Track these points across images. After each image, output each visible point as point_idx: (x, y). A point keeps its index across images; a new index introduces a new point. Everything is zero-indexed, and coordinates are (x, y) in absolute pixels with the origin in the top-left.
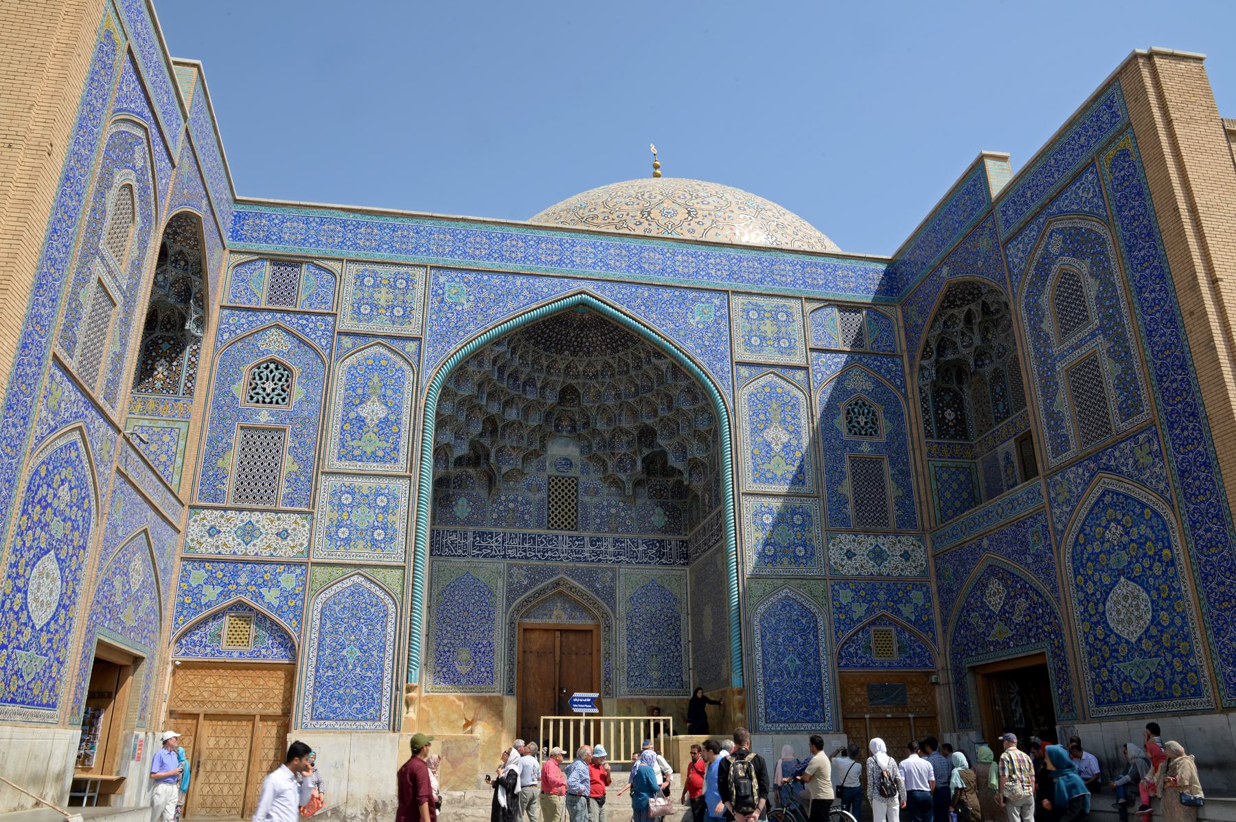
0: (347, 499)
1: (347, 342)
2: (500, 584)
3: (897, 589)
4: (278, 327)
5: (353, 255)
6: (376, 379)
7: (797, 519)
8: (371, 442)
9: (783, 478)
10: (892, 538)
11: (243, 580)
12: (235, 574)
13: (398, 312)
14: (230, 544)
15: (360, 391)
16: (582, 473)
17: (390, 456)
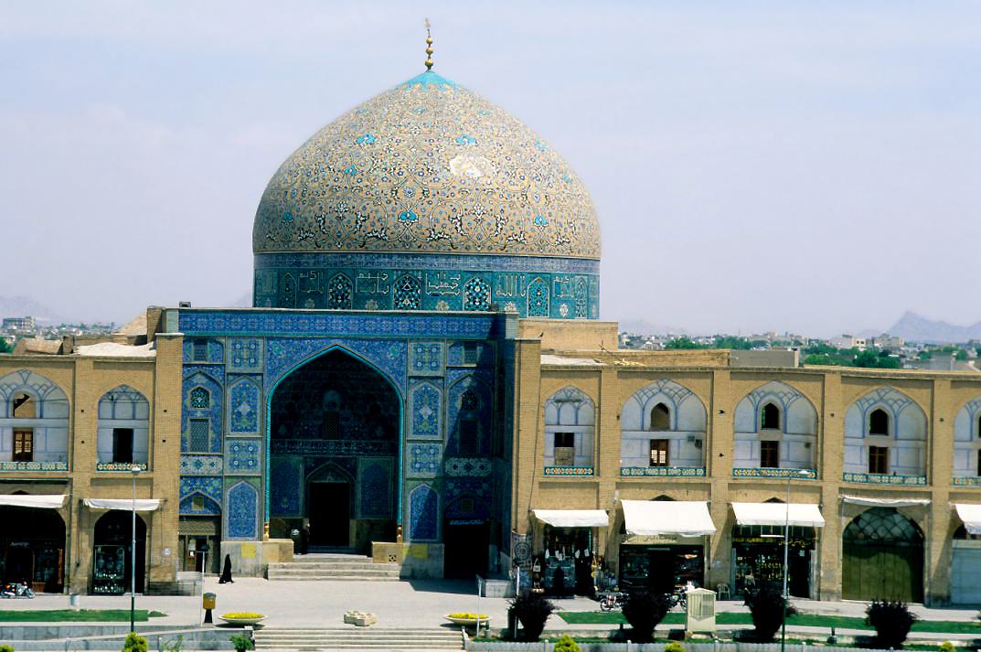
0: (236, 448)
1: (231, 378)
2: (301, 466)
3: (476, 482)
4: (200, 372)
5: (230, 333)
6: (245, 394)
7: (432, 451)
8: (245, 423)
9: (427, 432)
10: (476, 459)
11: (198, 483)
12: (195, 482)
13: (252, 361)
14: (192, 470)
15: (238, 400)
16: (341, 409)
17: (252, 429)
